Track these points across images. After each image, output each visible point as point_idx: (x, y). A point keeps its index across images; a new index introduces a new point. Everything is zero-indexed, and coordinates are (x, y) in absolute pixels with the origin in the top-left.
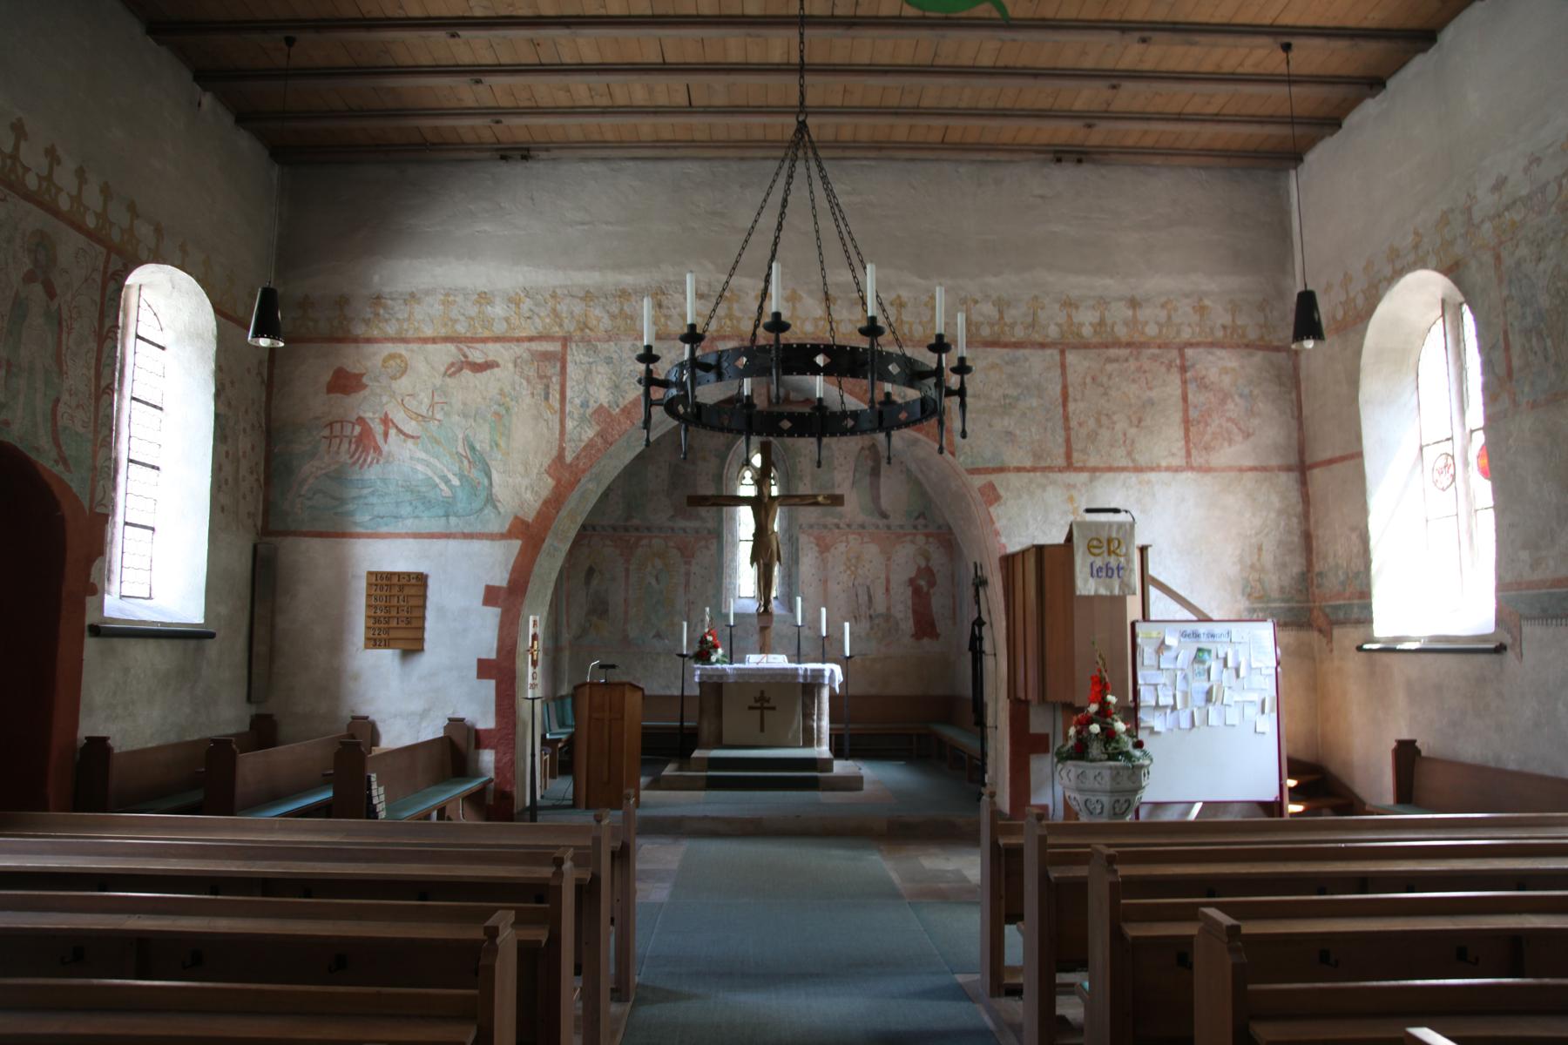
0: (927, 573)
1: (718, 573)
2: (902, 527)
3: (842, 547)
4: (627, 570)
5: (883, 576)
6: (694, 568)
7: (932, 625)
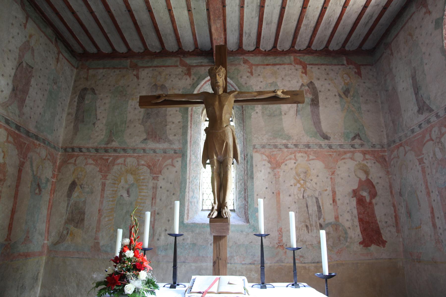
0: (368, 184)
1: (180, 189)
2: (341, 146)
3: (291, 164)
4: (104, 185)
5: (329, 189)
6: (161, 183)
7: (378, 232)
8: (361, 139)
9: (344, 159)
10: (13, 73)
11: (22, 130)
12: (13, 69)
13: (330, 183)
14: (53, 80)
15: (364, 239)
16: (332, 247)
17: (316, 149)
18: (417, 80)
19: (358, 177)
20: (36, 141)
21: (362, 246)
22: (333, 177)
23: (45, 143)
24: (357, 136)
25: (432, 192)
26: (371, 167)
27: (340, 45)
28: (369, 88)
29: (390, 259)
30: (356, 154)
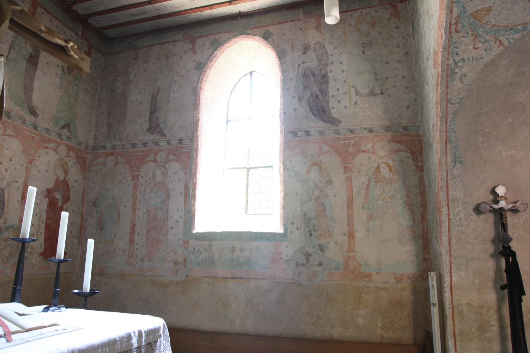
2: (47, 130)
5: (21, 181)
8: (70, 131)
9: (46, 147)
13: (24, 173)
15: (46, 249)
16: (7, 258)
17: (18, 122)
18: (158, 100)
19: (57, 175)
21: (41, 257)
22: (29, 166)
24: (66, 126)
25: (139, 209)
26: (72, 166)
27: (88, 12)
28: (92, 77)
29: (66, 273)
30: (60, 146)
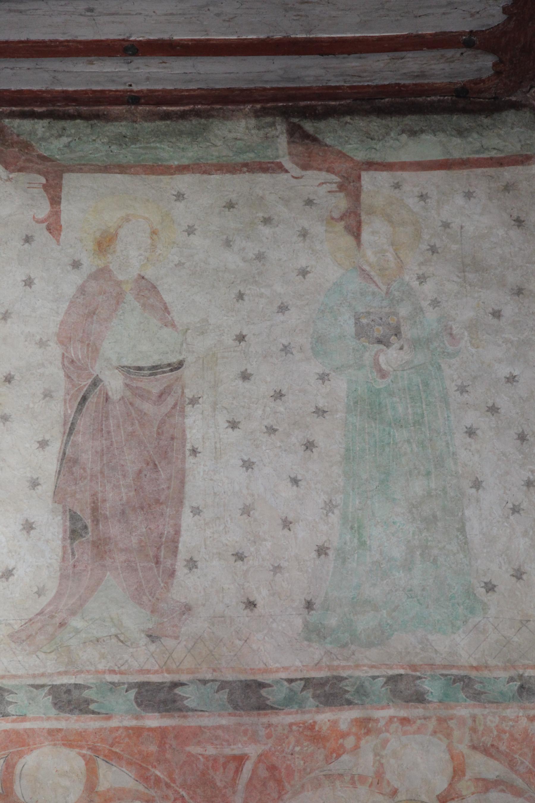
10: (49, 463)
11: (190, 696)
12: (43, 444)
14: (361, 332)
20: (324, 718)
23: (420, 698)
